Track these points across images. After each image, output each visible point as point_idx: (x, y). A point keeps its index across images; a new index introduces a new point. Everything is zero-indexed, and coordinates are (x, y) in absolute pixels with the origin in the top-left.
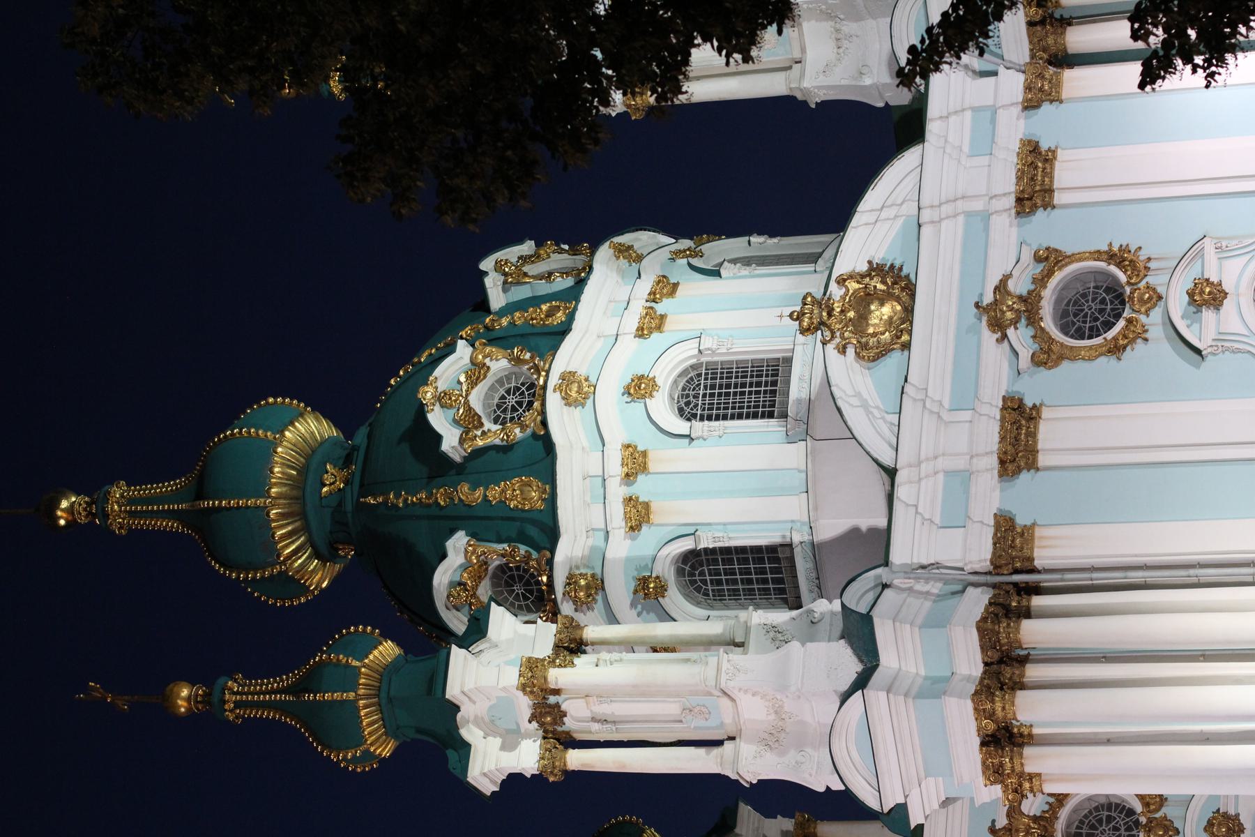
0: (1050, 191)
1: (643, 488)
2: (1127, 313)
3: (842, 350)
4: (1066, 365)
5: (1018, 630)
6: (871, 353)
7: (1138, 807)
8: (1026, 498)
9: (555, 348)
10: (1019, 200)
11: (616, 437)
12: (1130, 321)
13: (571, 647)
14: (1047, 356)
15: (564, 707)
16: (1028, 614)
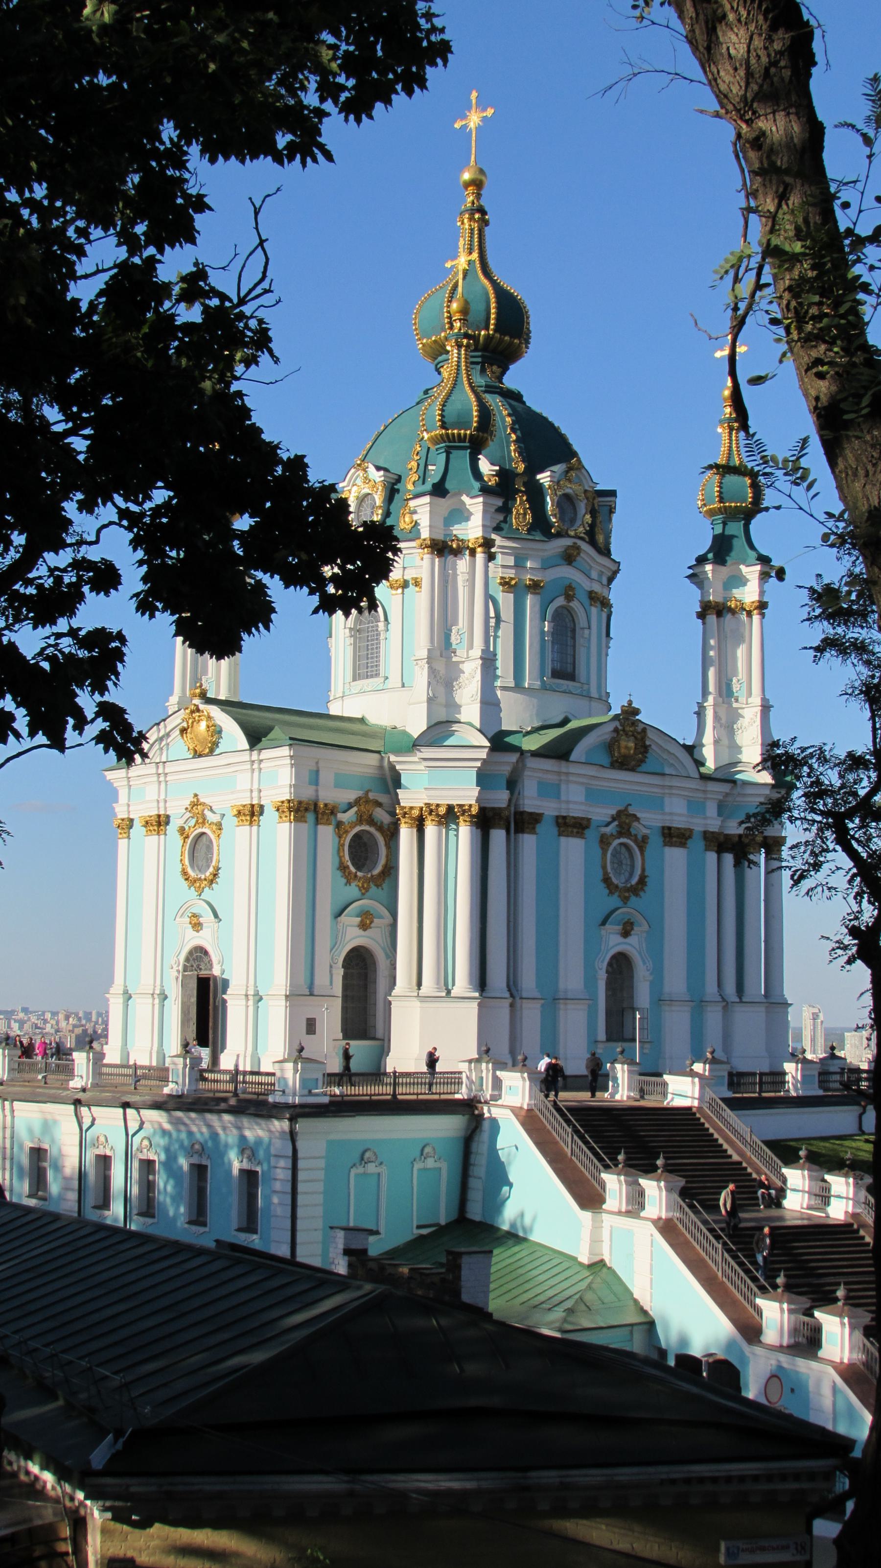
0: (671, 845)
3: (616, 730)
4: (600, 851)
5: (500, 828)
6: (610, 746)
10: (669, 828)
14: (604, 841)
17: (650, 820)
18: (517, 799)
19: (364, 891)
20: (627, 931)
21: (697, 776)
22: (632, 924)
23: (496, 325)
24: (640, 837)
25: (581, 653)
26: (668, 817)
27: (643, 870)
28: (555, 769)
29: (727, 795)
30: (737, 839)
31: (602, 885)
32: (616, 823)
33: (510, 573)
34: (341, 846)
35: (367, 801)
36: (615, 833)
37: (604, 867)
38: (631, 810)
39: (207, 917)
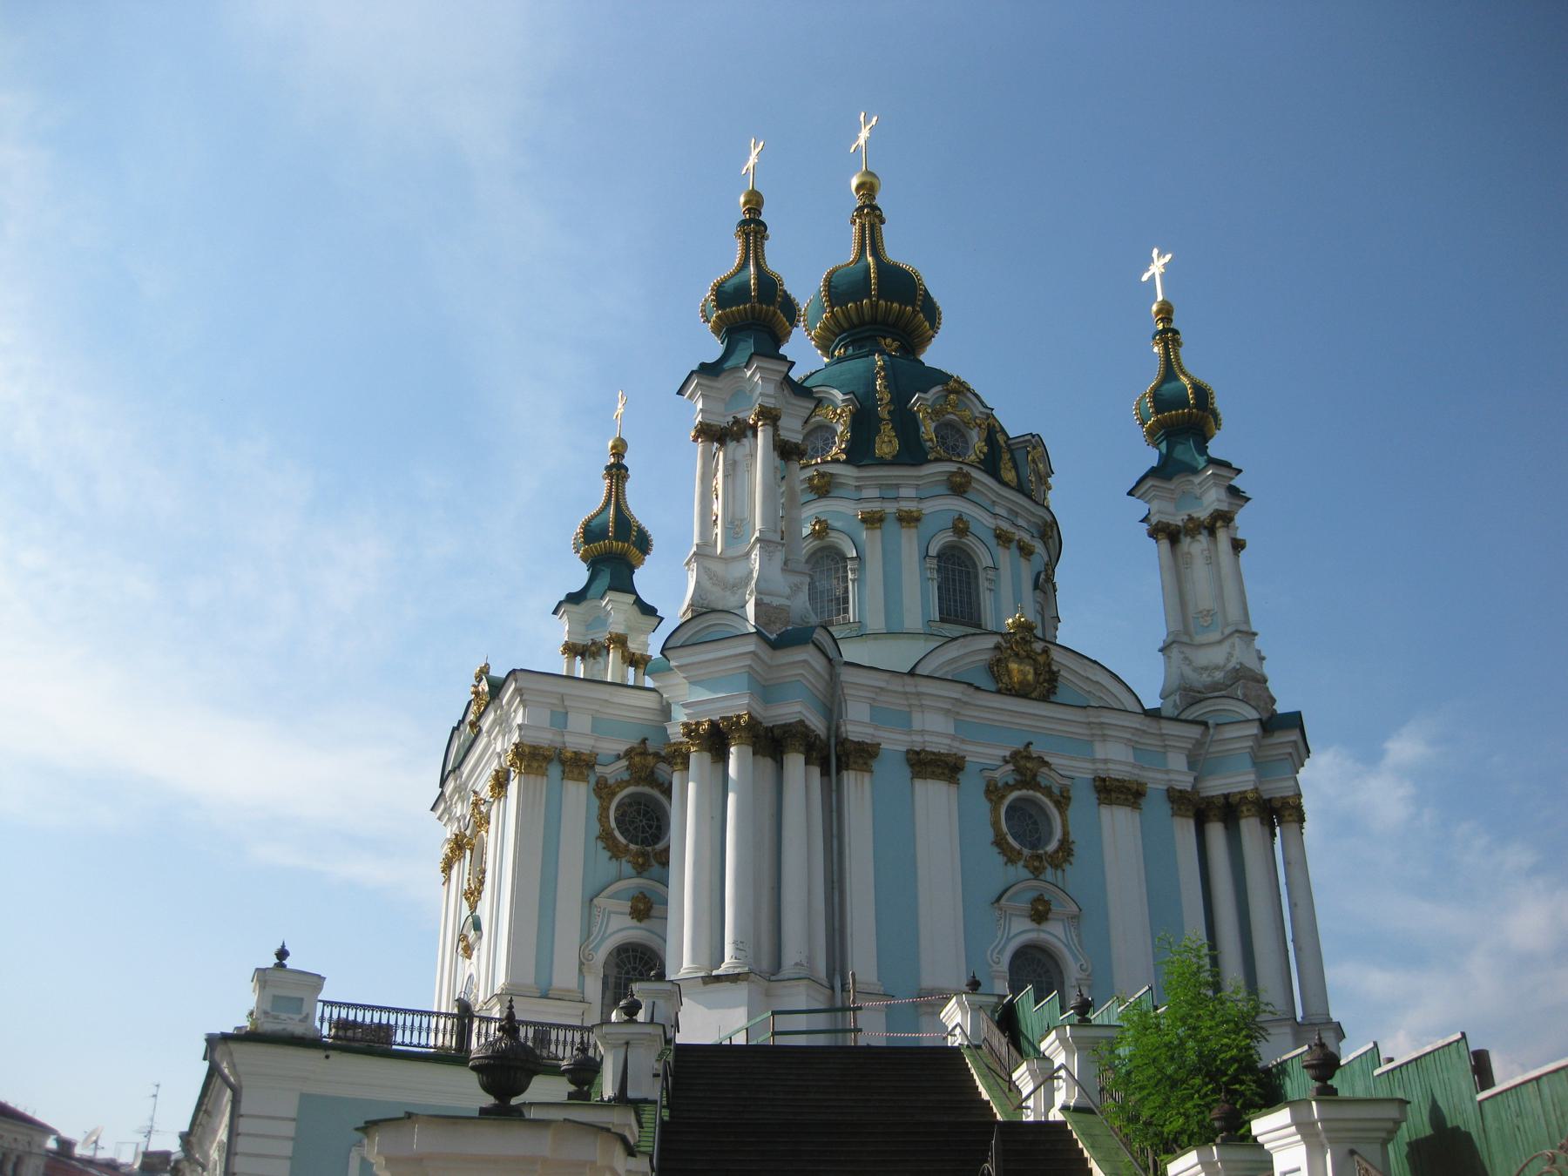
0: (1111, 803)
1: (891, 526)
2: (1026, 852)
3: (997, 647)
4: (984, 806)
6: (995, 669)
7: (660, 846)
8: (890, 769)
9: (986, 472)
10: (1104, 780)
11: (928, 507)
12: (1020, 853)
13: (786, 451)
14: (994, 792)
15: (745, 441)
16: (807, 763)
17: (1071, 767)
18: (838, 728)
19: (641, 869)
20: (1040, 912)
21: (1139, 710)
22: (1047, 903)
23: (879, 290)
24: (1056, 791)
25: (987, 601)
26: (1100, 766)
27: (1066, 833)
28: (900, 689)
29: (1199, 744)
30: (1222, 800)
31: (996, 850)
32: (1010, 767)
33: (876, 506)
34: (604, 811)
35: (644, 753)
36: (1011, 782)
37: (995, 824)
38: (1035, 750)
39: (472, 935)
